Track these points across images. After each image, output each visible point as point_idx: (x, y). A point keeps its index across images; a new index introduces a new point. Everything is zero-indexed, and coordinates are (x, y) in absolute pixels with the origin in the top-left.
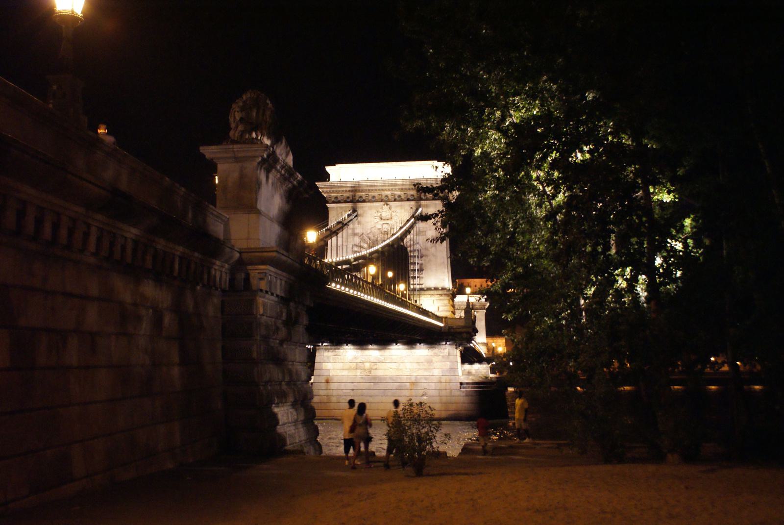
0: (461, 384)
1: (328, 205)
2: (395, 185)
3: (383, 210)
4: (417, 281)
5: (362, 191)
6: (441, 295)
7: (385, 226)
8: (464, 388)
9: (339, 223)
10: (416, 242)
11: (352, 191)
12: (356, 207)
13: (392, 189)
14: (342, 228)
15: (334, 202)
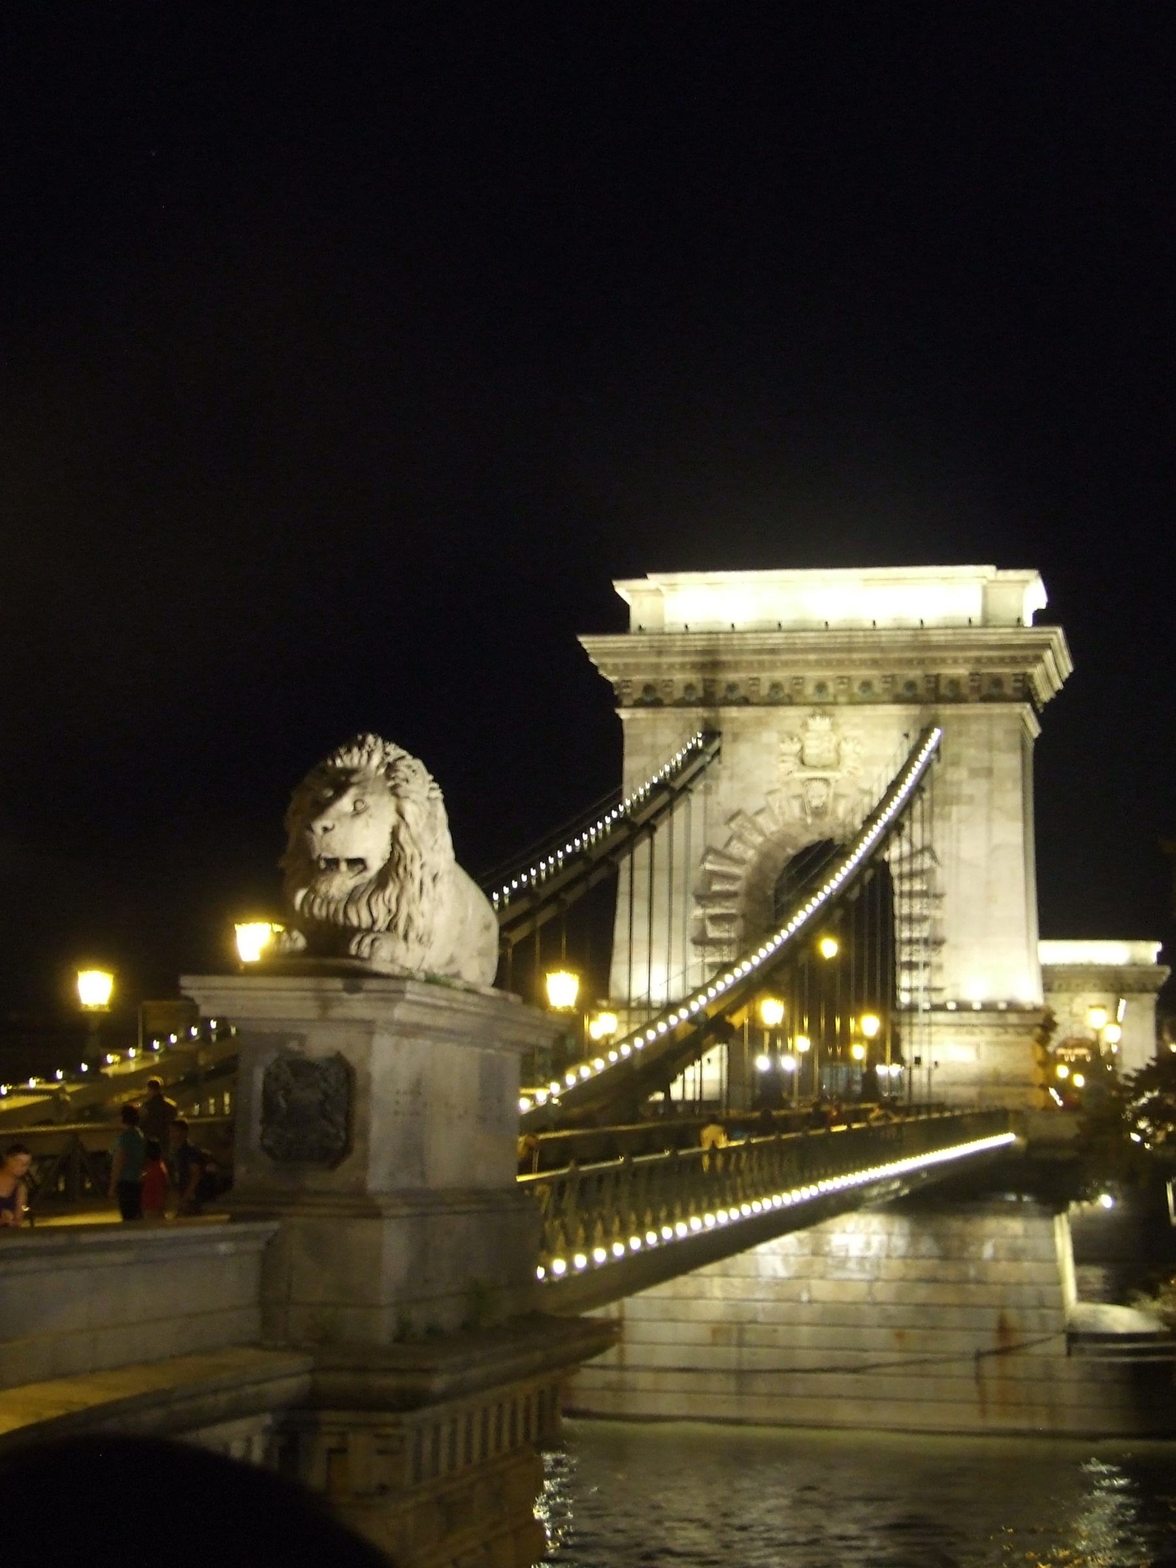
1: (624, 714)
2: (850, 649)
3: (808, 735)
4: (919, 979)
5: (735, 666)
6: (1005, 1027)
7: (818, 787)
8: (1082, 1351)
9: (657, 789)
10: (919, 846)
12: (718, 720)
13: (840, 663)
14: (669, 807)
15: (639, 704)
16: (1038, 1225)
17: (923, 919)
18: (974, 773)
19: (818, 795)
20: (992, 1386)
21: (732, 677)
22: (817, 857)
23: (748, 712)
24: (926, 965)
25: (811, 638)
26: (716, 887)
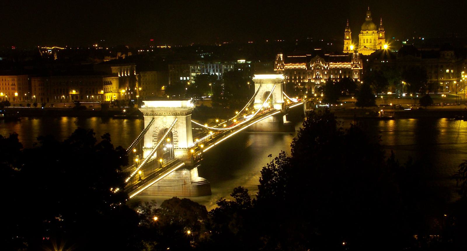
0: (192, 182)
1: (144, 116)
4: (176, 145)
11: (152, 112)
16: (188, 171)
17: (176, 139)
18: (181, 123)
19: (165, 126)
20: (184, 188)
21: (155, 112)
22: (166, 130)
23: (157, 116)
24: (176, 144)
25: (163, 109)
26: (155, 135)
